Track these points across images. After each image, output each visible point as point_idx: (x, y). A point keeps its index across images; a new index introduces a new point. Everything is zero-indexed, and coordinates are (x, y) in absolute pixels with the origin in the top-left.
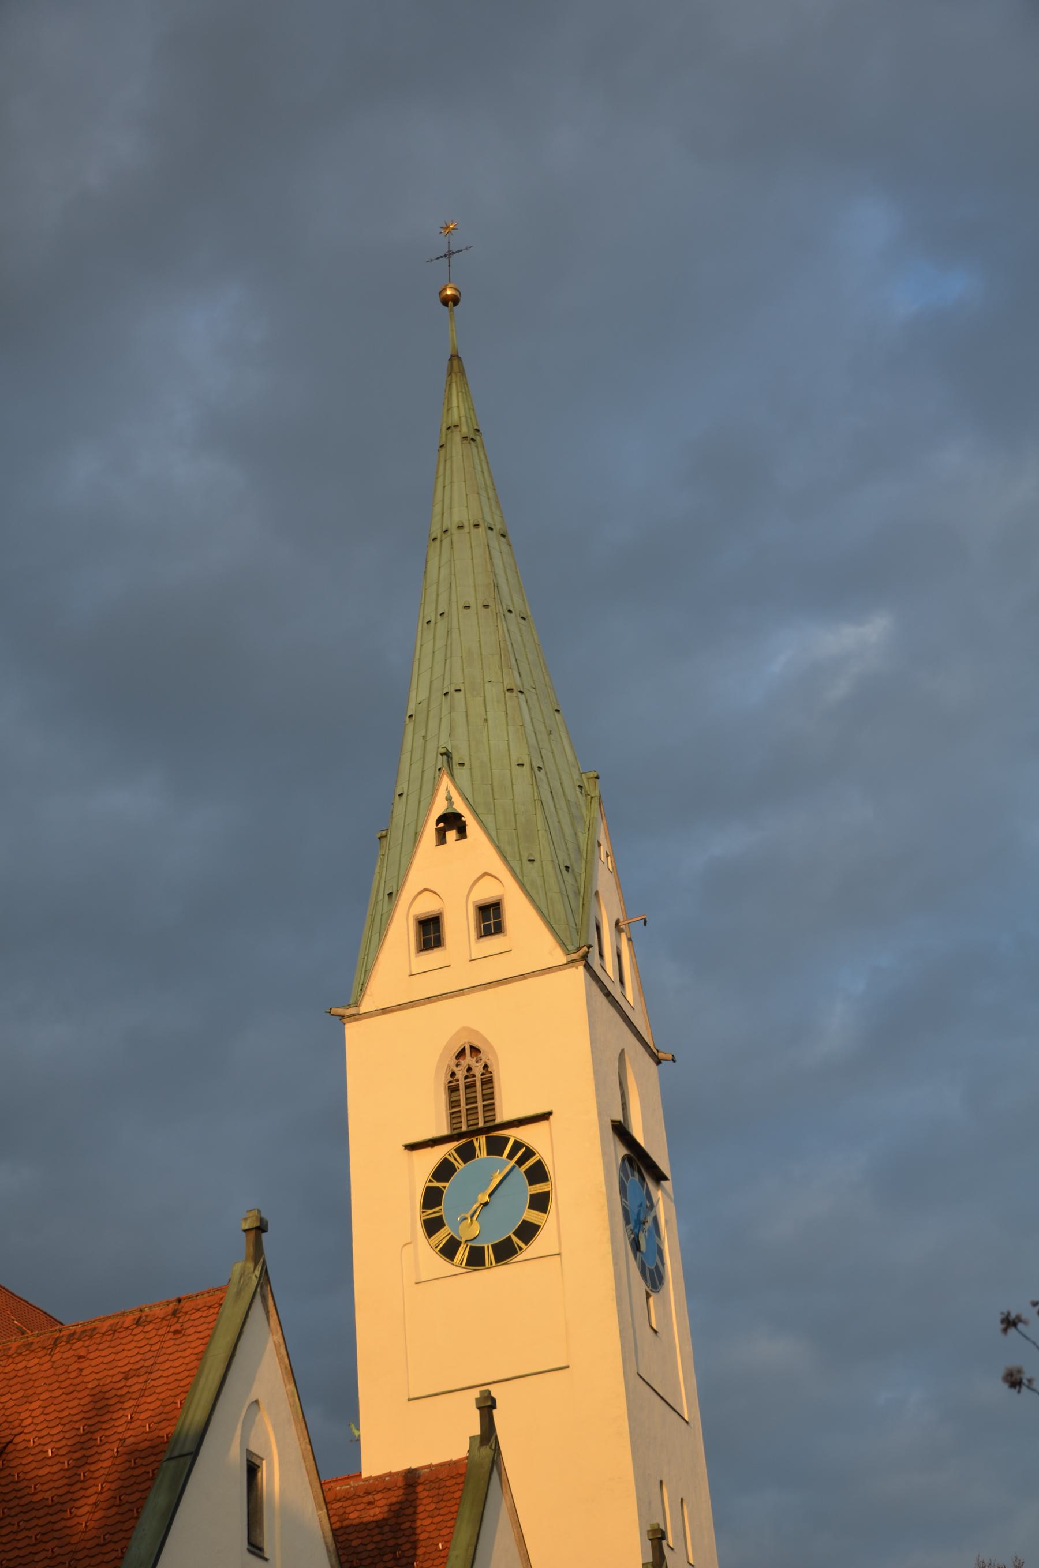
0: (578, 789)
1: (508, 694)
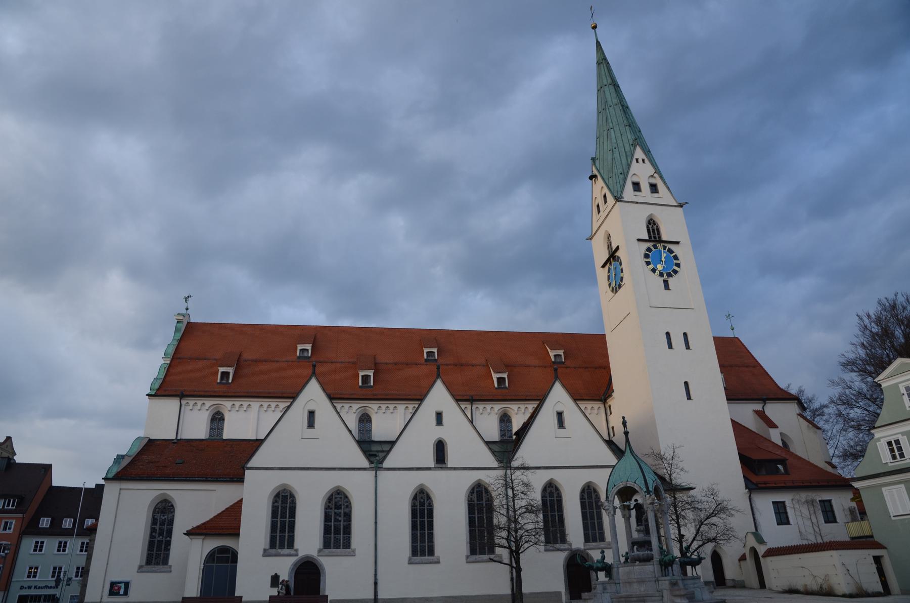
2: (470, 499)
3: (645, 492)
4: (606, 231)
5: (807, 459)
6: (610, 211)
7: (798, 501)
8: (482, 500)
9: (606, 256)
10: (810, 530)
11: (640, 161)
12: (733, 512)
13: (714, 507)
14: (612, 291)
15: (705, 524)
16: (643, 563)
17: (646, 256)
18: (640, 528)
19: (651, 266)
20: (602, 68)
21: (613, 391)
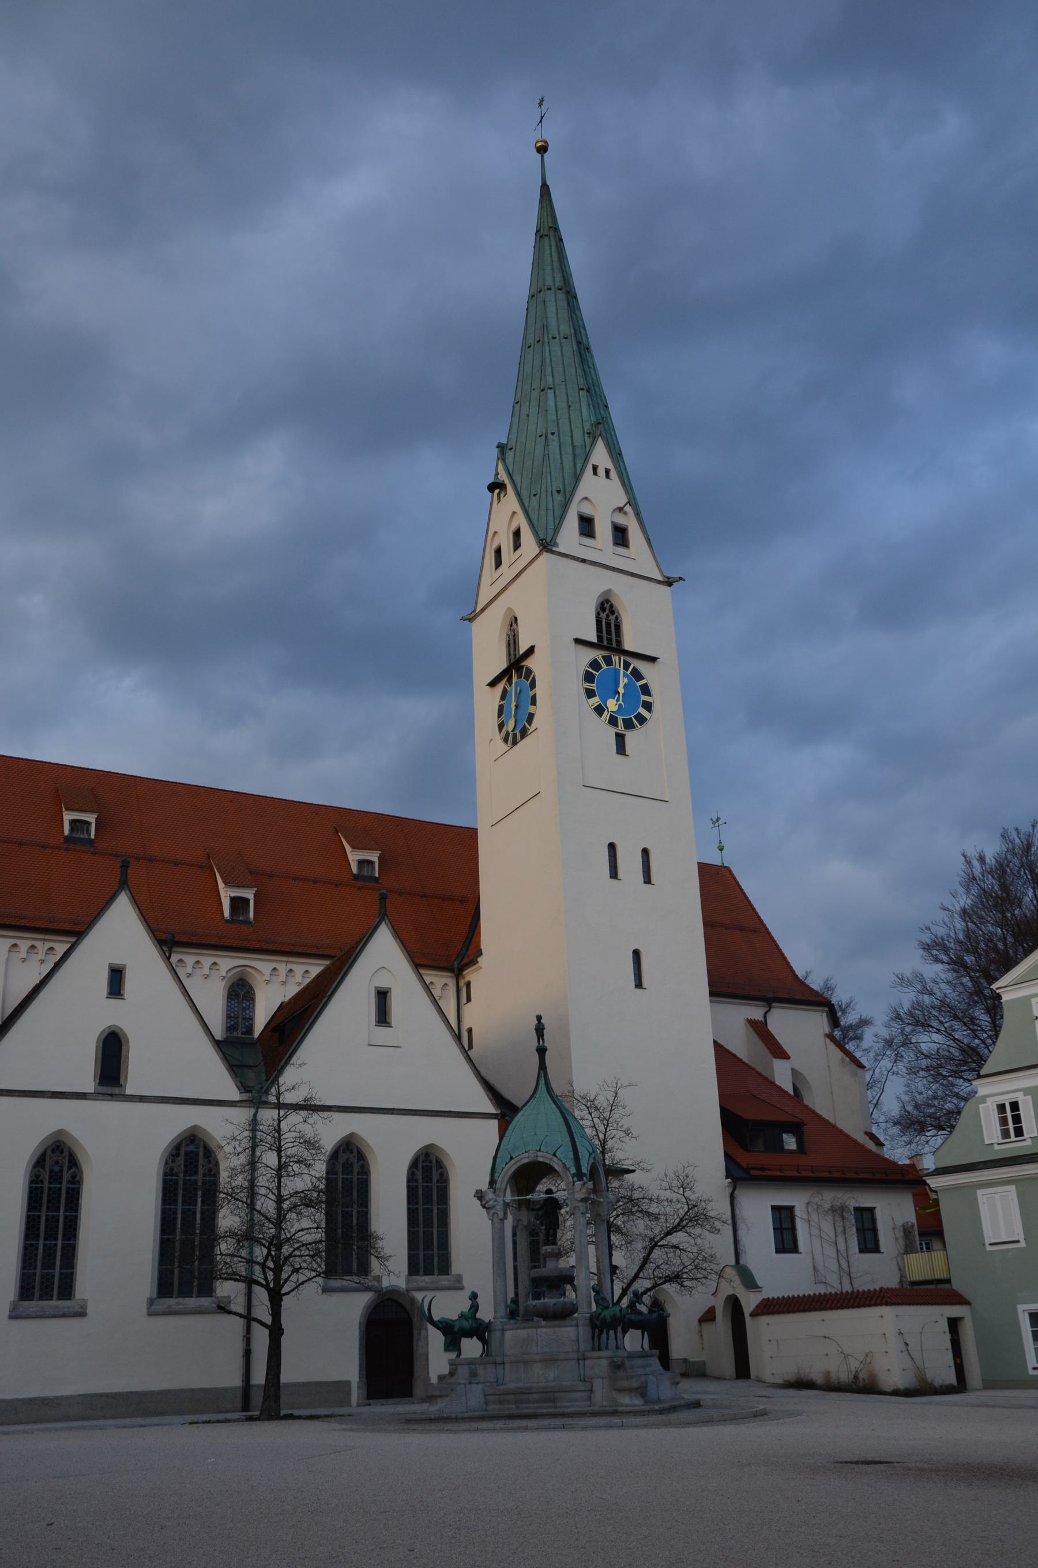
0: (586, 435)
1: (542, 393)
2: (168, 1170)
3: (573, 1176)
4: (510, 609)
5: (832, 1120)
6: (525, 569)
7: (818, 1207)
8: (196, 1173)
9: (501, 664)
10: (833, 1266)
11: (601, 472)
12: (718, 1224)
13: (682, 1212)
14: (506, 740)
15: (662, 1246)
16: (557, 1322)
17: (589, 677)
18: (553, 1250)
19: (595, 701)
20: (547, 248)
21: (480, 953)
